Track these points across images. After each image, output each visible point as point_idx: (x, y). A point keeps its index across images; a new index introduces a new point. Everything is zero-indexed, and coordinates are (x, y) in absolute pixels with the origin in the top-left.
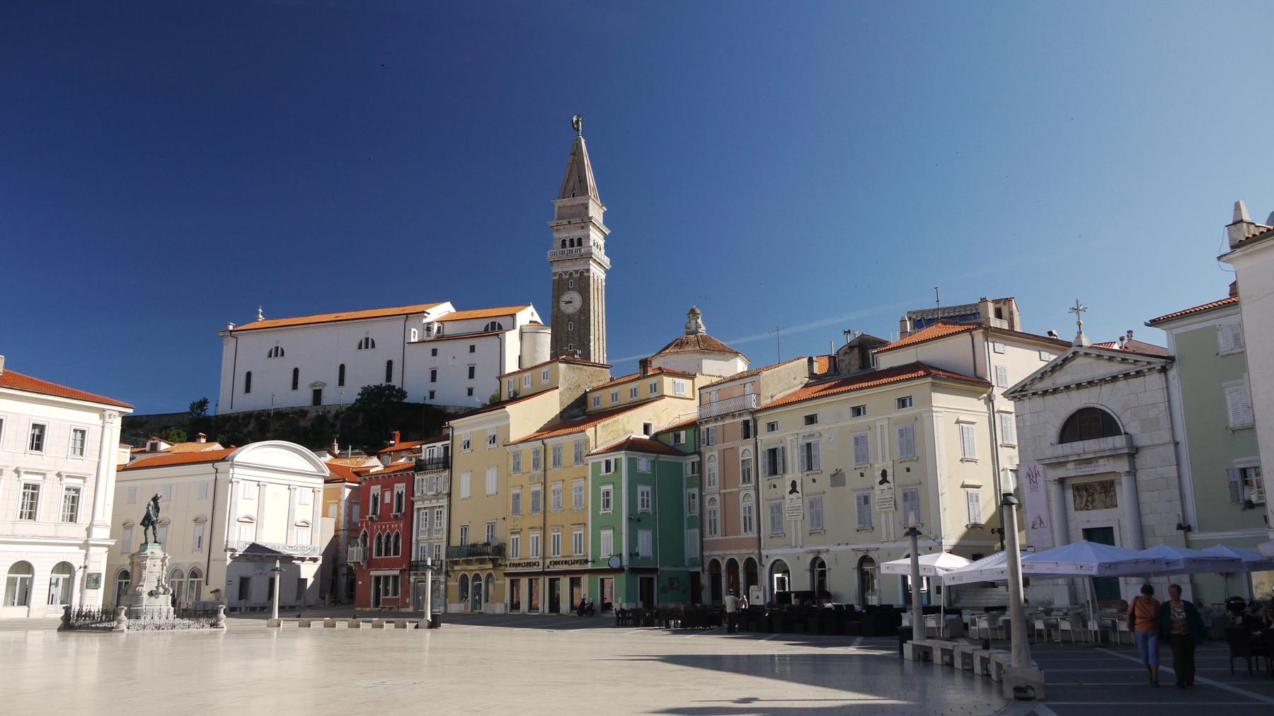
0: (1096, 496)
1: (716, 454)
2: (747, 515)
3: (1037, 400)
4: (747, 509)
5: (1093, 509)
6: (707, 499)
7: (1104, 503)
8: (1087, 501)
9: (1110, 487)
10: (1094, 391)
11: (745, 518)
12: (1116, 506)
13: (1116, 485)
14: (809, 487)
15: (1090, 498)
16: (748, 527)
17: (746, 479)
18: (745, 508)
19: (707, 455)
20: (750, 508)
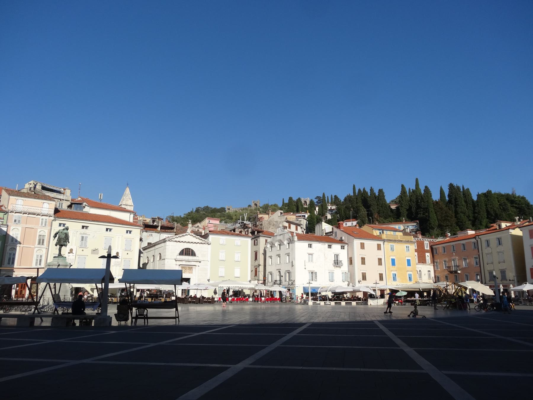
0: (187, 270)
1: (20, 228)
2: (39, 259)
3: (175, 243)
4: (39, 256)
5: (186, 273)
6: (8, 248)
7: (189, 272)
8: (184, 271)
9: (191, 268)
10: (192, 244)
11: (37, 260)
12: (192, 273)
13: (193, 268)
14: (80, 252)
15: (185, 270)
16: (38, 264)
17: (41, 242)
18: (37, 256)
19: (12, 228)
20: (41, 256)
